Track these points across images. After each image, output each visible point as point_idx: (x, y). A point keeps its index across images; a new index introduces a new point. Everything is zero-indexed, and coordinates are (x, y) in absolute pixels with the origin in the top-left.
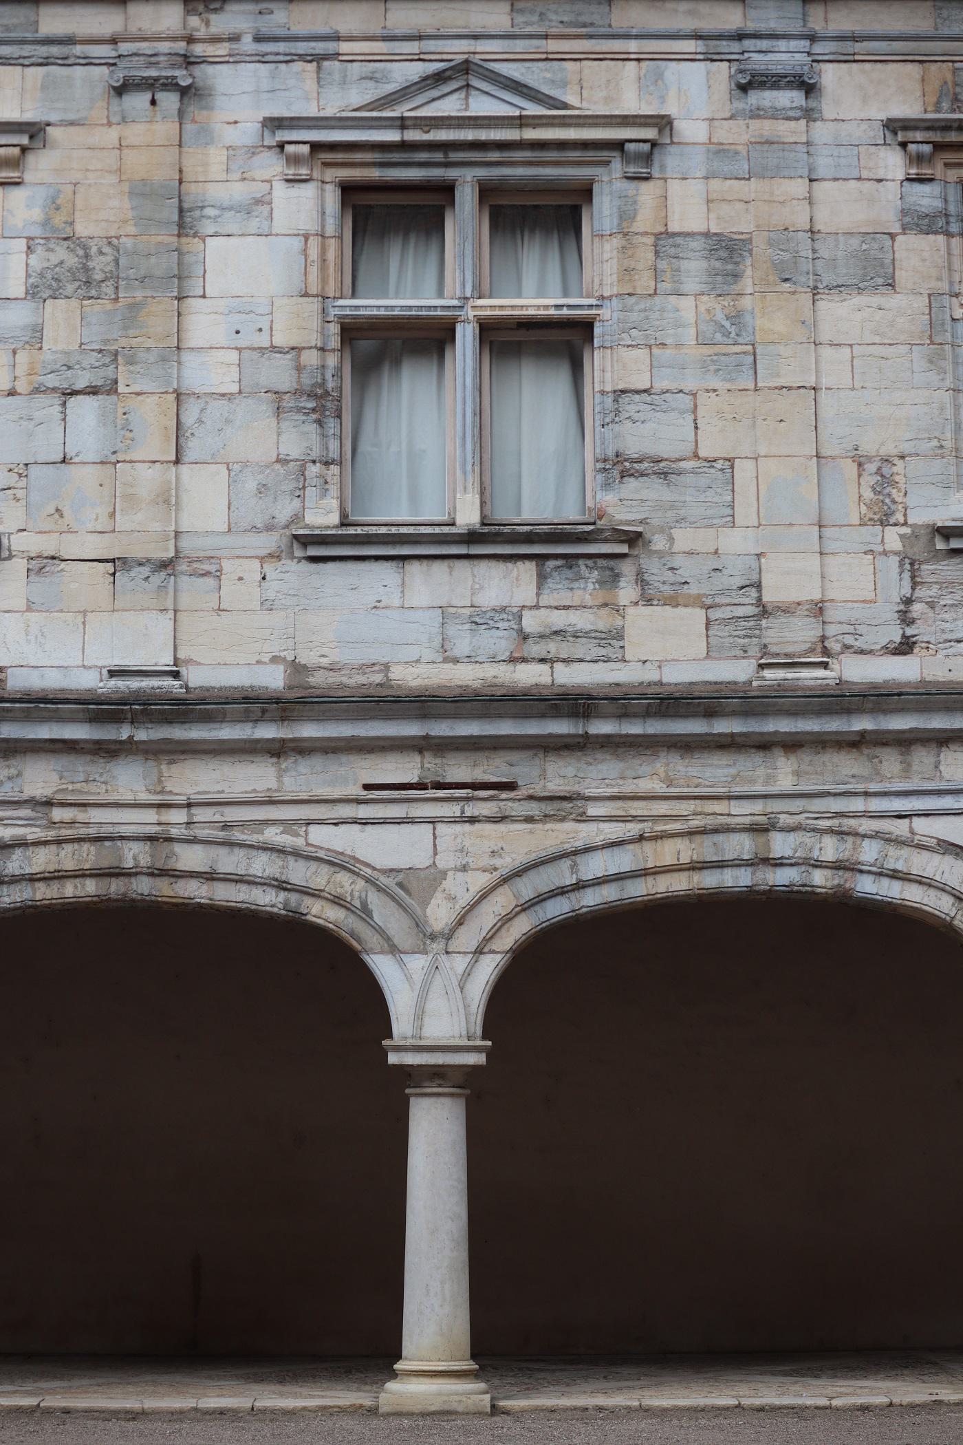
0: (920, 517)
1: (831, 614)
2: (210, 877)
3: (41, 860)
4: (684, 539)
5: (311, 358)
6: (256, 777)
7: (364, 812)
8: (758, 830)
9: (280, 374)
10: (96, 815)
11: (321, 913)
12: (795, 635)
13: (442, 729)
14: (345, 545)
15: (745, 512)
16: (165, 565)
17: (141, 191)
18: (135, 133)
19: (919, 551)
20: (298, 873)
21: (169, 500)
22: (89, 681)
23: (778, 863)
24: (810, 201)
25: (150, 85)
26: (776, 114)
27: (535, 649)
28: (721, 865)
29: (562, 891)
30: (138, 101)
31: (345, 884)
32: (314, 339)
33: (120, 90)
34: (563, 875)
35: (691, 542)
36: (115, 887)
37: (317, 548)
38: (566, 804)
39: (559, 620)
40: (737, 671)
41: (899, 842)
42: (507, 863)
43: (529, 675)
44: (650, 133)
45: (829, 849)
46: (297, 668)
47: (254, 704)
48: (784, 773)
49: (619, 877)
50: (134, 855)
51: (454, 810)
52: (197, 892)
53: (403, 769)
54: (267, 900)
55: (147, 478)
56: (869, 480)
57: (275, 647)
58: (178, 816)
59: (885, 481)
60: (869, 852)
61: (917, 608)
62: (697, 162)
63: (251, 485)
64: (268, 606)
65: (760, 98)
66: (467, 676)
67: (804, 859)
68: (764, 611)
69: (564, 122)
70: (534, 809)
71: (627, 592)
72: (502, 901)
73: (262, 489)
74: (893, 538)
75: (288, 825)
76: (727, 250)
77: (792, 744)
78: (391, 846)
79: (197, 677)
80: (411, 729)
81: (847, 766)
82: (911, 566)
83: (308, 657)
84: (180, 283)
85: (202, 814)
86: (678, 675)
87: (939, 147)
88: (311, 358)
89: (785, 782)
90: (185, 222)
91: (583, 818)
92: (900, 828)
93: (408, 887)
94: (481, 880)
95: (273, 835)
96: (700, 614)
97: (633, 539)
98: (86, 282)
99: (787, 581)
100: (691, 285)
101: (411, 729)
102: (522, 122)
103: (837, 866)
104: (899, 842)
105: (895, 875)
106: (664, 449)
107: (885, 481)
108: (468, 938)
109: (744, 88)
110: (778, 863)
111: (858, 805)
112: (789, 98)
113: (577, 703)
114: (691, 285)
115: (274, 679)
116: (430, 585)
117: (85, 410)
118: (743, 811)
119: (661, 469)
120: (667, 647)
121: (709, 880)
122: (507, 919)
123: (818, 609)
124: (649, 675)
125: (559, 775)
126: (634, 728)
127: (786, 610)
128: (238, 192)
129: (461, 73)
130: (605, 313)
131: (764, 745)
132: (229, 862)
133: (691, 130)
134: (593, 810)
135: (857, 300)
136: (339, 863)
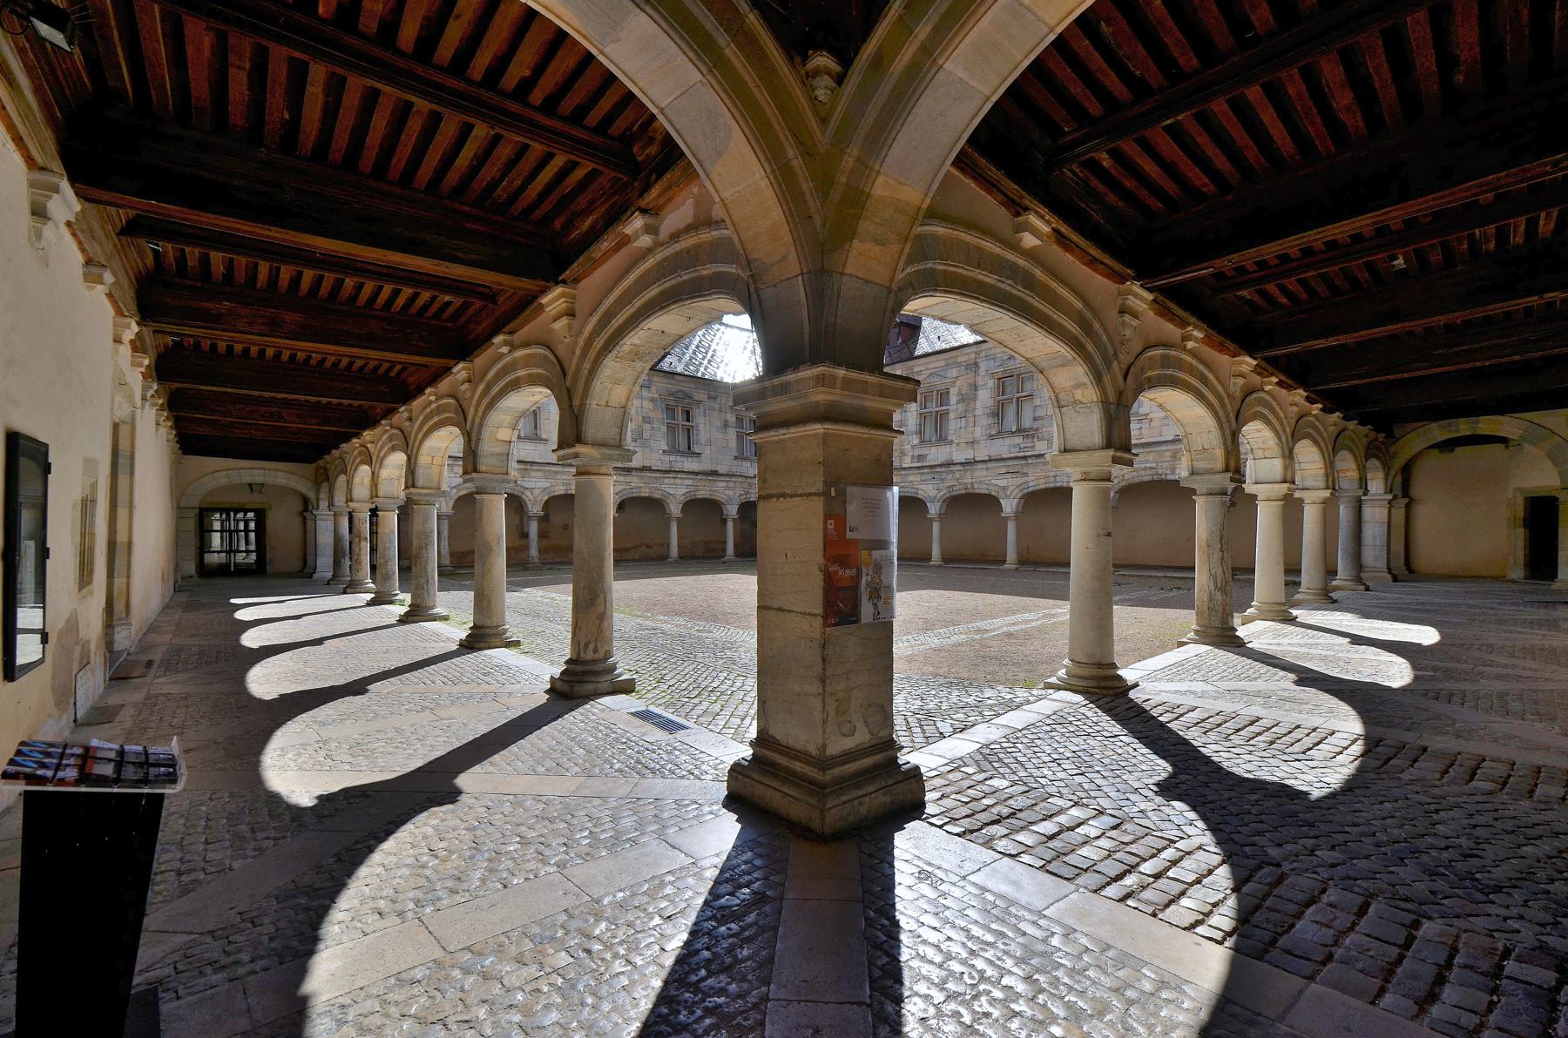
37: (991, 437)
38: (1026, 474)
78: (1002, 483)
84: (975, 398)
90: (976, 389)
93: (1004, 488)
113: (1025, 458)
119: (1042, 418)
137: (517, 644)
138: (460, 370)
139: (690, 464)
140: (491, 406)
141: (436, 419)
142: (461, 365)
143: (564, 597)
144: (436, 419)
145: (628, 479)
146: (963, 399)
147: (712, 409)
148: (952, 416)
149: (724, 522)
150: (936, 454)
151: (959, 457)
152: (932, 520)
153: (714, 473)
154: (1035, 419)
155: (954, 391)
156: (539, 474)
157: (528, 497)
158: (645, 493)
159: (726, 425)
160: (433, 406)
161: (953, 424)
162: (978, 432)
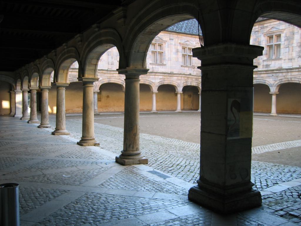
10: (287, 77)
16: (291, 59)
18: (291, 28)
47: (296, 68)
50: (290, 79)
55: (290, 53)
58: (292, 76)
63: (297, 53)
84: (293, 39)
85: (293, 76)
90: (293, 34)
95: (298, 77)
132: (295, 79)
137: (99, 144)
138: (78, 37)
139: (161, 69)
140: (90, 51)
141: (67, 55)
142: (78, 35)
143: (116, 129)
144: (67, 55)
148: (282, 47)
151: (286, 65)
152: (271, 95)
155: (283, 35)
159: (177, 51)
160: (66, 50)
161: (283, 50)
162: (295, 55)
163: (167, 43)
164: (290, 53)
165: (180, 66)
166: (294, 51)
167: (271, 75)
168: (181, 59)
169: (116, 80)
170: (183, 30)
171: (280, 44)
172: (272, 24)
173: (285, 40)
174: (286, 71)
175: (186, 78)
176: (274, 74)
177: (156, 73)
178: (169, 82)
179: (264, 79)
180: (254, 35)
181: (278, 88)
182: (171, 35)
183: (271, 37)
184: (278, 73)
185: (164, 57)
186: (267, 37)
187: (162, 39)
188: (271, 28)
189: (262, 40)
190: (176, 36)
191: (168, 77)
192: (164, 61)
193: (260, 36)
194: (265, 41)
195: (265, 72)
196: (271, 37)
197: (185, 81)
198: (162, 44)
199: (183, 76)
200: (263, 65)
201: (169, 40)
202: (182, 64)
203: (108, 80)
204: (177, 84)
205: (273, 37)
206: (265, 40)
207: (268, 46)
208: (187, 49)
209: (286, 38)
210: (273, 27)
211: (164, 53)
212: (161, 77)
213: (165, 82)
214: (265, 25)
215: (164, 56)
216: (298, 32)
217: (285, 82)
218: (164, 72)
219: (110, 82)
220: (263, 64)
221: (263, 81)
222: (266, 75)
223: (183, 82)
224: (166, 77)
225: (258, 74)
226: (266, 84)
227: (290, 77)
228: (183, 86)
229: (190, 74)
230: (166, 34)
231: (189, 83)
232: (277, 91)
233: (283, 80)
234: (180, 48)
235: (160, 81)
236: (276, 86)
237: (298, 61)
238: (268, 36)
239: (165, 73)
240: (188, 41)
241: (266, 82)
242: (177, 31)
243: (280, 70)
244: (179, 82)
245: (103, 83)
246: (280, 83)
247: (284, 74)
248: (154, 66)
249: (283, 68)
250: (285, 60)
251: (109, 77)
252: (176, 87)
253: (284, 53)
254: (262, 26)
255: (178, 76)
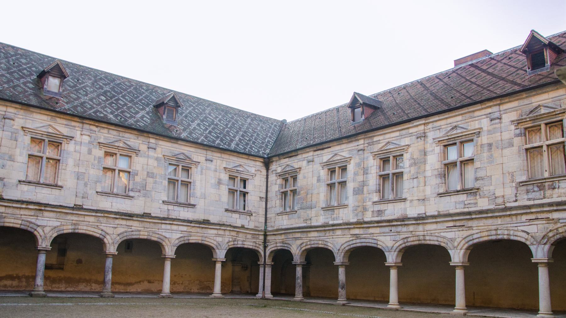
0: (518, 181)
1: (505, 197)
2: (430, 240)
3: (412, 239)
4: (485, 188)
5: (440, 170)
6: (434, 226)
7: (446, 230)
8: (496, 230)
9: (436, 173)
10: (417, 233)
11: (442, 244)
12: (500, 201)
13: (454, 218)
14: (447, 193)
15: (493, 183)
16: (423, 200)
17: (420, 151)
18: (419, 144)
19: (518, 186)
20: (439, 239)
21: (424, 191)
22: (416, 216)
23: (499, 235)
24: (501, 136)
25: (420, 137)
26: (496, 124)
27: (466, 206)
28: (491, 235)
29: (471, 240)
30: (419, 139)
31: (445, 241)
32: (440, 167)
33: (417, 138)
34: (471, 238)
35: (486, 189)
36: (420, 242)
37: (440, 195)
38: (470, 228)
39: (469, 202)
40: (492, 207)
41: (516, 231)
42: (464, 237)
43: (466, 210)
44: (478, 131)
45: (506, 232)
46: (439, 212)
48: (499, 221)
49: (478, 238)
50: (421, 238)
51: (457, 230)
52: (428, 242)
53: (451, 224)
54: (436, 243)
55: (421, 188)
56: (510, 176)
57: (436, 209)
58: (426, 232)
59: (513, 176)
60: (512, 233)
61: (518, 195)
62: (486, 133)
64: (435, 204)
65: (493, 122)
66: (458, 211)
67: (503, 234)
68: (496, 198)
69: (469, 131)
70: (467, 229)
71: (478, 197)
72: (463, 242)
73: (435, 188)
74: (514, 184)
75: (438, 233)
76: (490, 145)
77: (500, 217)
78: (450, 235)
79: (428, 214)
80: (450, 219)
81: (508, 219)
82: (517, 188)
83: (440, 210)
84: (425, 162)
85: (428, 232)
86: (484, 208)
87: (518, 123)
88: (440, 170)
89: (499, 223)
90: (425, 154)
91: (473, 230)
92: (516, 228)
93: (452, 240)
94: (460, 239)
95: (437, 234)
96: (487, 199)
97: (478, 189)
98: (415, 164)
99: (499, 193)
100: (485, 151)
101: (450, 219)
102: (462, 133)
103: (507, 235)
104: (516, 231)
105: (516, 236)
106: (482, 176)
107: (513, 176)
108: (459, 247)
109: (491, 121)
110: (499, 235)
111: (509, 225)
112: (498, 121)
113: (469, 213)
114: (485, 151)
115: (436, 213)
116: (454, 198)
117: (415, 180)
118: (494, 227)
120: (483, 204)
121: (490, 238)
122: (464, 244)
123: (503, 196)
124: (481, 208)
125: (470, 223)
126: (477, 216)
127: (498, 197)
128: (431, 149)
129: (455, 127)
130: (475, 157)
131: (497, 217)
132: (431, 238)
133: (485, 129)
134: (474, 228)
135: (508, 149)
136: (444, 237)
139: (185, 214)
145: (130, 223)
146: (415, 163)
147: (207, 169)
148: (405, 177)
149: (215, 263)
150: (393, 211)
151: (413, 211)
152: (389, 267)
153: (206, 222)
154: (477, 179)
155: (406, 156)
156: (52, 215)
157: (39, 233)
158: (144, 235)
159: (220, 182)
162: (429, 191)
163: (199, 166)
164: (421, 188)
165: (224, 210)
166: (427, 184)
167: (387, 229)
168: (225, 196)
169: (89, 228)
170: (233, 146)
171: (402, 172)
172: (387, 136)
173: (410, 166)
174: (414, 222)
175: (234, 234)
176: (393, 229)
177: (174, 220)
178: (200, 238)
179: (375, 238)
180: (357, 157)
181: (401, 254)
182: (209, 153)
183: (385, 161)
184: (399, 225)
185: (192, 191)
186: (378, 160)
187: (190, 159)
188: (386, 145)
189: (369, 165)
190: (219, 155)
191: (199, 230)
192: (191, 198)
193: (367, 158)
194: (375, 167)
195: (376, 225)
196: (385, 161)
197: (231, 239)
198: (191, 168)
199: (228, 229)
200: (373, 212)
201: (205, 162)
202: (227, 208)
203: (73, 227)
204: (215, 243)
205: (389, 160)
206: (375, 164)
207: (381, 176)
208: (238, 180)
209: (413, 161)
210: (389, 142)
211: (192, 184)
212: (185, 228)
213: (191, 238)
214: (375, 139)
215: (192, 189)
216: (434, 150)
217: (413, 243)
218: (191, 219)
219: (77, 231)
220: (372, 210)
221: (373, 241)
222: (377, 230)
223: (227, 240)
224: (194, 229)
225: (363, 228)
226: (379, 247)
227: (422, 233)
228: (228, 249)
229: (243, 227)
230: (199, 151)
231: (240, 242)
232: (399, 260)
233: (409, 240)
234: (225, 177)
235: (182, 235)
236: (397, 250)
237: (435, 204)
238: (381, 159)
239: (191, 222)
240: (240, 165)
241: (379, 243)
242: (221, 147)
243: (403, 220)
244: (219, 239)
245: (62, 232)
246: (404, 245)
247: (411, 228)
248: (171, 207)
249: (409, 216)
250: (411, 201)
251: (74, 222)
252: (214, 249)
253: (409, 189)
254: (370, 141)
255: (218, 227)
